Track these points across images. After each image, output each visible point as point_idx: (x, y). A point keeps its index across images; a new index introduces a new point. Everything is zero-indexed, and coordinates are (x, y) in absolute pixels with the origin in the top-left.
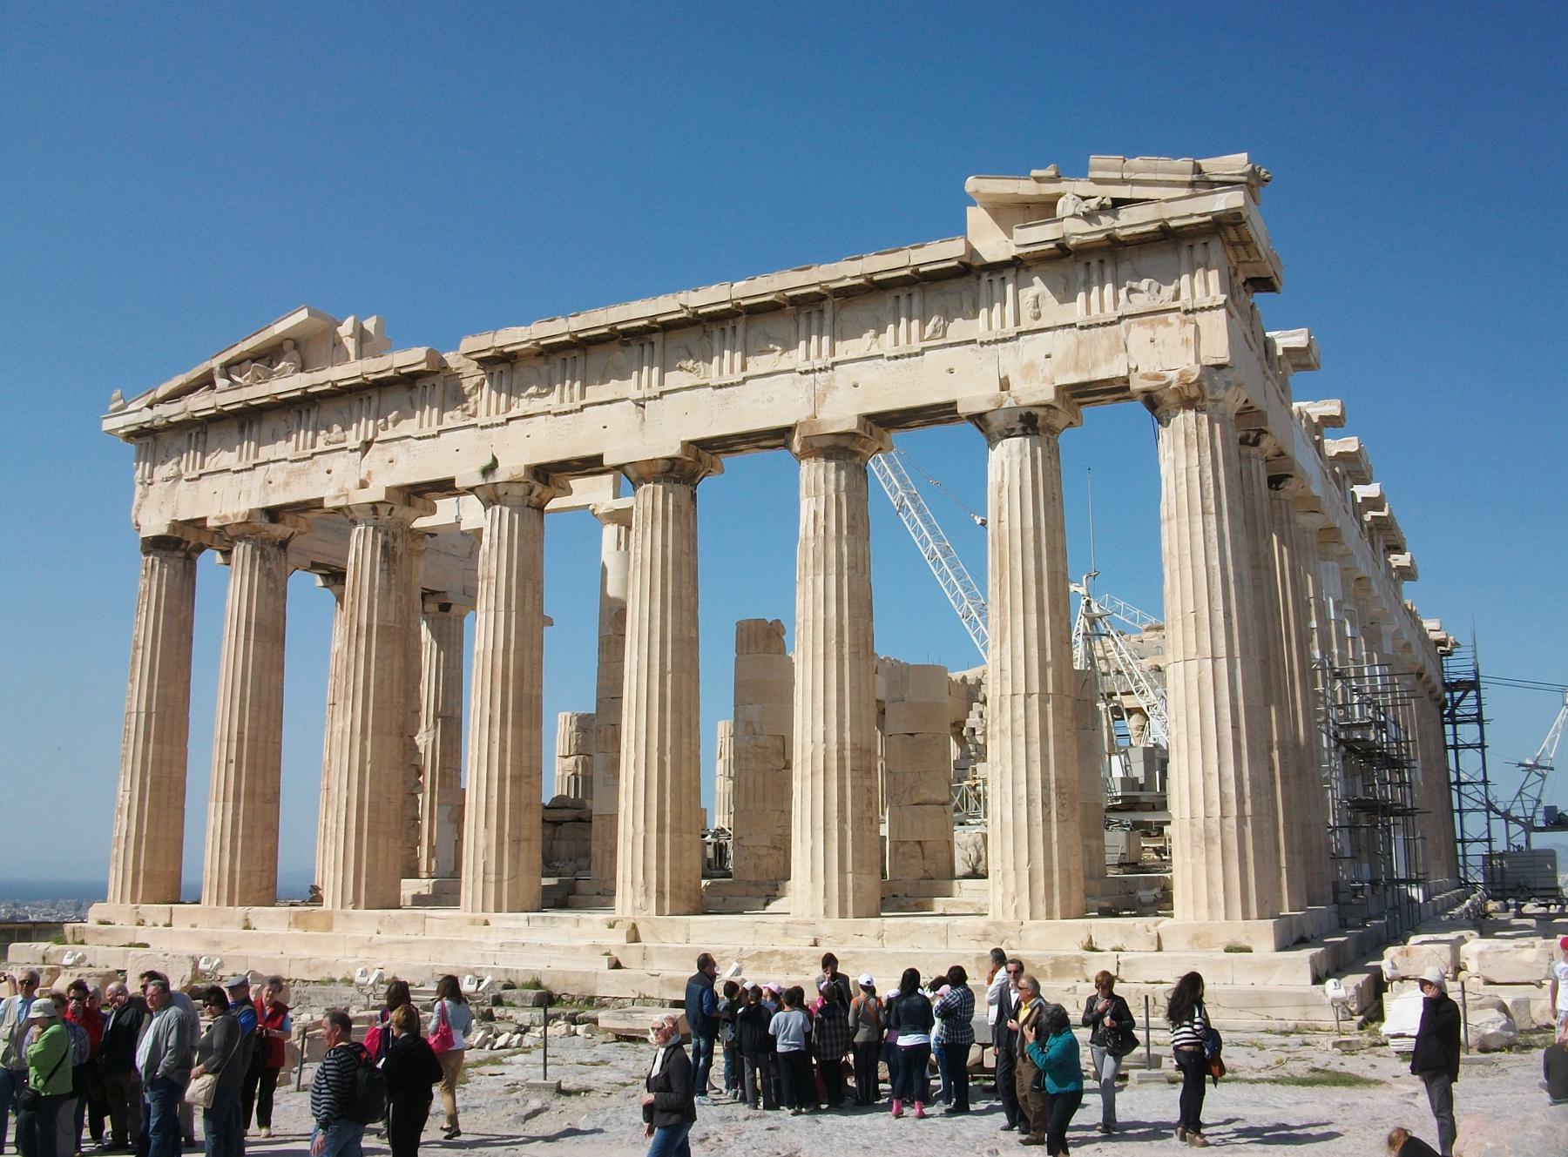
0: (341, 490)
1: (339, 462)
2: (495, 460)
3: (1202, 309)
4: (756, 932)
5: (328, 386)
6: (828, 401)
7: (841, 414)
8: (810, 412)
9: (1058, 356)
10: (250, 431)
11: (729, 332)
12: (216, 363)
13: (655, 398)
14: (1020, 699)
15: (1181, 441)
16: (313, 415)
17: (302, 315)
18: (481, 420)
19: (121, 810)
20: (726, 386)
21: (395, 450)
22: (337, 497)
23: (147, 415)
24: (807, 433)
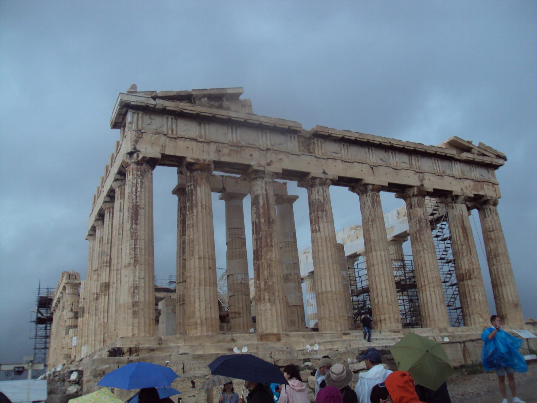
1: (256, 154)
5: (258, 122)
21: (282, 156)
22: (260, 166)
23: (152, 102)
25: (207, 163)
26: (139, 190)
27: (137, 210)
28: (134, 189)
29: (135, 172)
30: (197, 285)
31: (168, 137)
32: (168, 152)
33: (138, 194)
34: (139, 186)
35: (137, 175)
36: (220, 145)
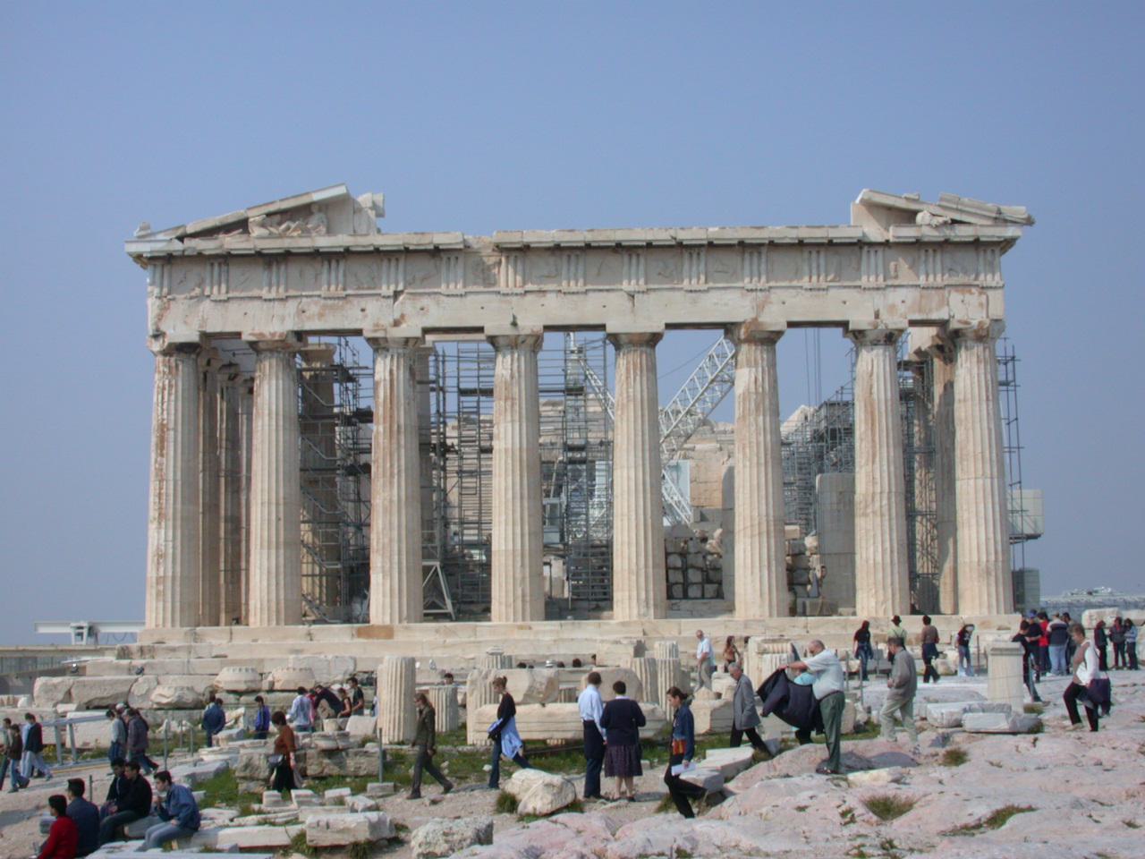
0: (377, 325)
1: (372, 306)
2: (514, 317)
3: (991, 288)
4: (726, 627)
5: (371, 248)
6: (766, 310)
7: (773, 318)
8: (753, 315)
9: (909, 302)
10: (279, 269)
11: (695, 256)
12: (255, 216)
13: (643, 292)
14: (885, 495)
15: (975, 359)
16: (342, 265)
17: (341, 191)
18: (502, 287)
19: (160, 556)
20: (696, 291)
21: (425, 301)
22: (375, 331)
24: (753, 328)
25: (277, 338)
26: (166, 399)
27: (163, 431)
28: (160, 396)
29: (161, 368)
30: (259, 547)
31: (215, 301)
32: (212, 328)
33: (165, 405)
34: (166, 392)
35: (164, 373)
36: (304, 300)
